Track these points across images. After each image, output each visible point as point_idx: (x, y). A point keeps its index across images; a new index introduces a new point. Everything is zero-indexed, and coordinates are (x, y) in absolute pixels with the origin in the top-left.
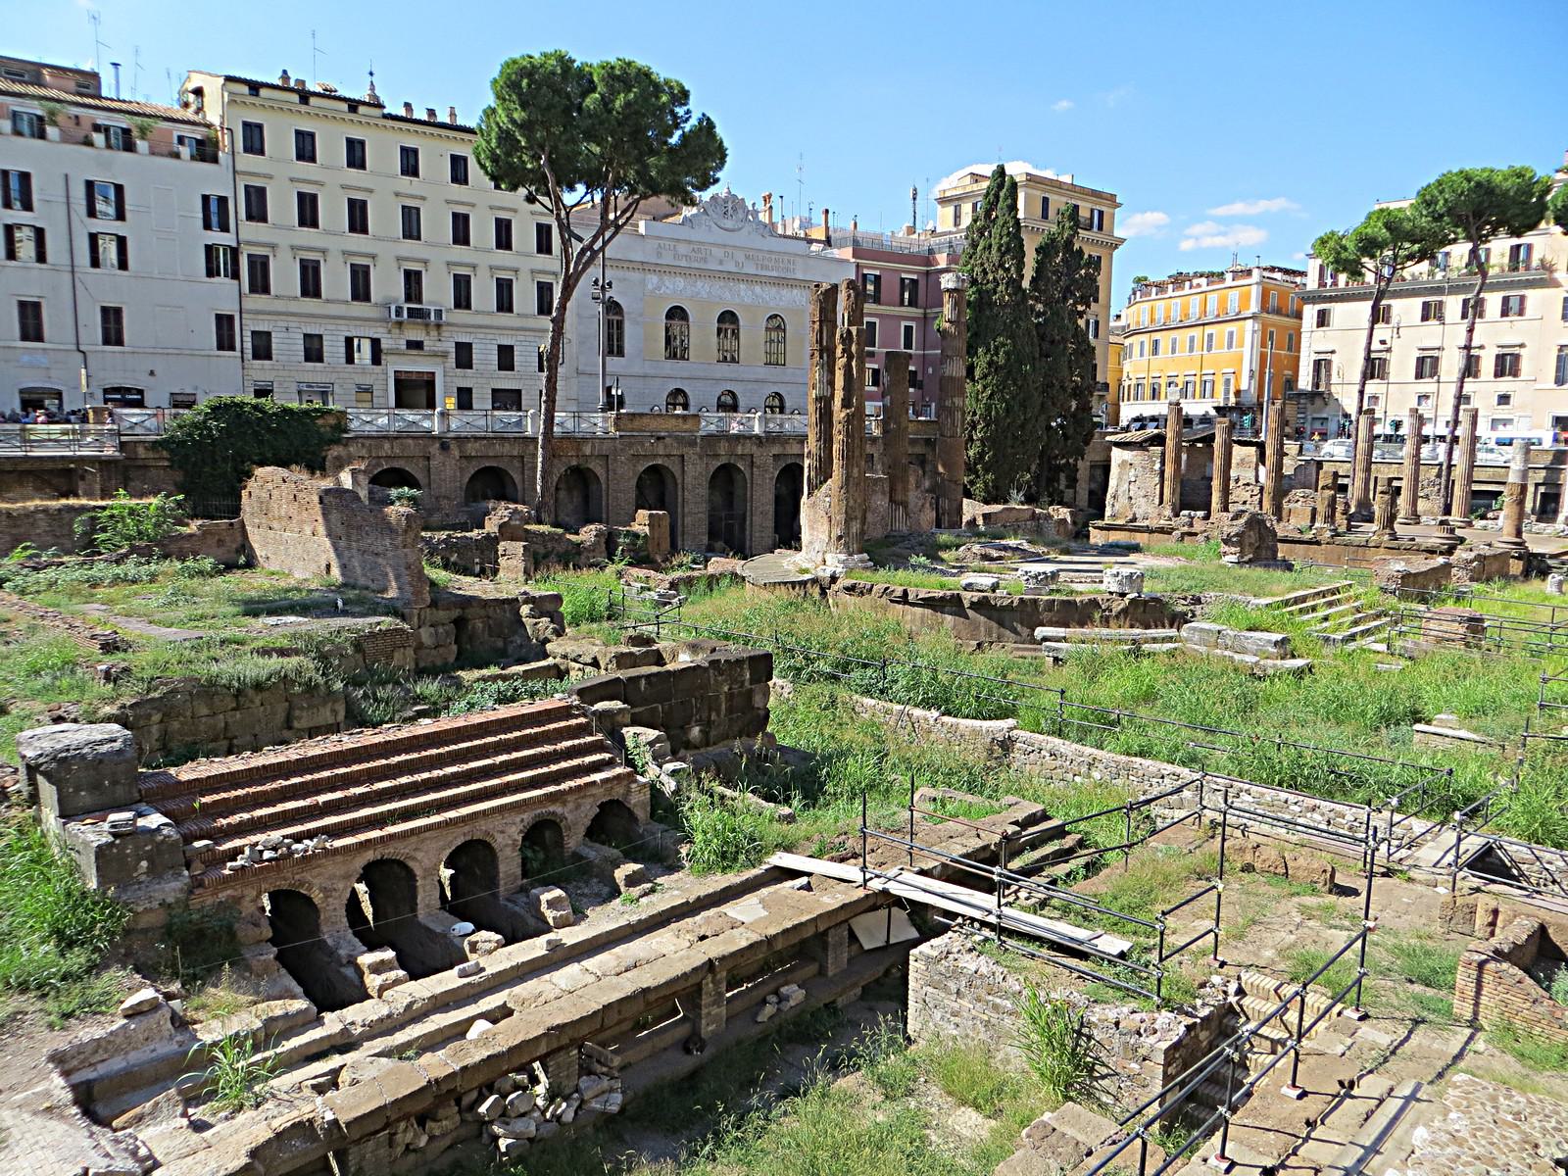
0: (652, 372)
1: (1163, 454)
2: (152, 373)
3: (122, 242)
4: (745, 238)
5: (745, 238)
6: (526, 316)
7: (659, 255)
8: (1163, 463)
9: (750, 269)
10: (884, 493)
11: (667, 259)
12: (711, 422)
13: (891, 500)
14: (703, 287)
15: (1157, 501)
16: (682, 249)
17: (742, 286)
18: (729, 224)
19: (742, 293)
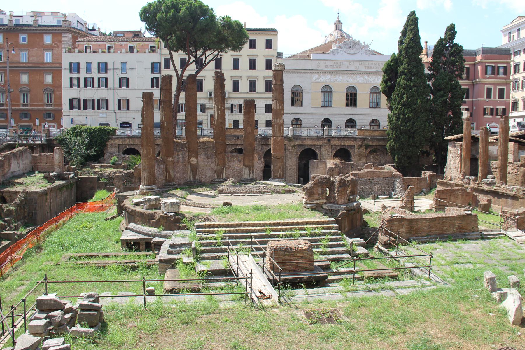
0: (315, 112)
1: (461, 145)
2: (134, 118)
3: (128, 79)
4: (361, 56)
5: (361, 56)
6: (261, 93)
7: (319, 66)
8: (461, 150)
9: (362, 68)
10: (240, 162)
11: (322, 67)
12: (288, 131)
13: (244, 165)
14: (339, 78)
15: (459, 171)
16: (329, 63)
17: (358, 76)
18: (352, 51)
19: (358, 79)
